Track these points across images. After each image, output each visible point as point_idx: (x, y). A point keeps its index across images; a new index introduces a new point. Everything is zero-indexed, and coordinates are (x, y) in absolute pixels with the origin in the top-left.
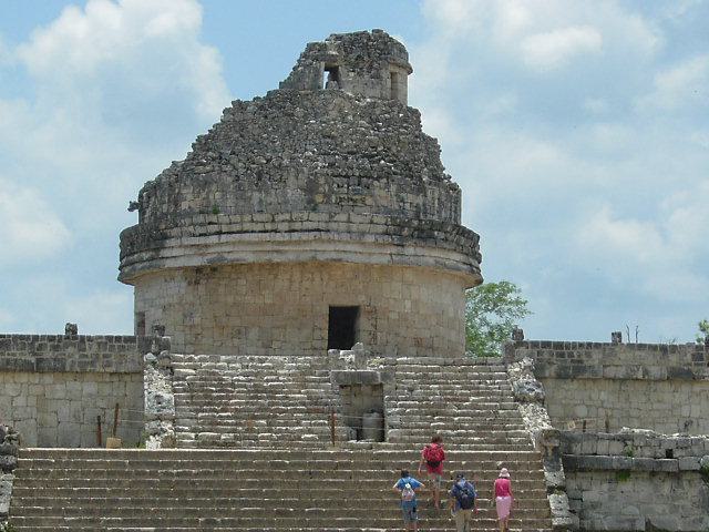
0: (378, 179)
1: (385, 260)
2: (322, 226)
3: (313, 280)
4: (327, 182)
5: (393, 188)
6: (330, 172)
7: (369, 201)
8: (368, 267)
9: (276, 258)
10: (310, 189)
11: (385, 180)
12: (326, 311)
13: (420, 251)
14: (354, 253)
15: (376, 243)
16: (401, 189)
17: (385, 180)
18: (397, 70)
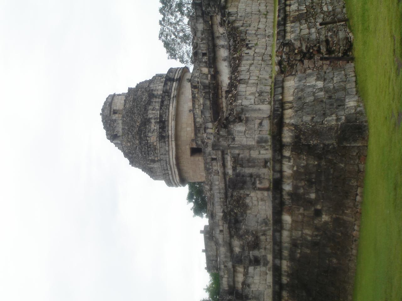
0: (147, 140)
1: (174, 143)
2: (165, 162)
3: (183, 161)
4: (151, 157)
5: (150, 134)
6: (147, 156)
7: (155, 144)
8: (177, 146)
10: (153, 161)
11: (148, 138)
12: (192, 158)
13: (170, 128)
15: (169, 146)
17: (148, 138)
18: (112, 110)
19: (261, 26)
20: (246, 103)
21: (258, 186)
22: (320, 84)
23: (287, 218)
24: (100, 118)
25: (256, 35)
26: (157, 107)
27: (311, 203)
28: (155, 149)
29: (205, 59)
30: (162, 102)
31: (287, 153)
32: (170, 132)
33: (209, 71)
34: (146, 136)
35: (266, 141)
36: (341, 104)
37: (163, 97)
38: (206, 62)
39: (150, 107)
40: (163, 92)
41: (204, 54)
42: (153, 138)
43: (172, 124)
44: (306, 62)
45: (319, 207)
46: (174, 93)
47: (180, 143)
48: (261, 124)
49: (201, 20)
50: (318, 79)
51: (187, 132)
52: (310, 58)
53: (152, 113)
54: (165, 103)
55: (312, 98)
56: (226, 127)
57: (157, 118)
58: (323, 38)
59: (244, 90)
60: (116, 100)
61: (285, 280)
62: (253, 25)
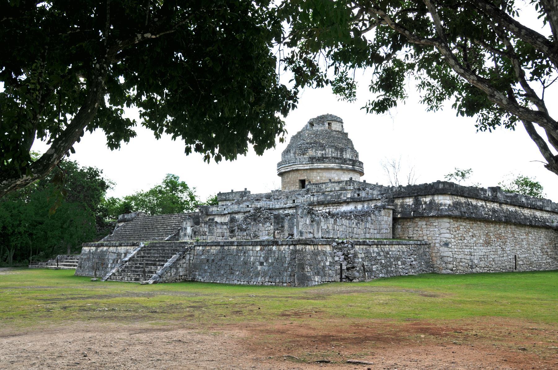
1: (308, 167)
5: (314, 150)
8: (307, 169)
9: (287, 170)
10: (295, 153)
12: (298, 181)
13: (318, 164)
14: (301, 167)
16: (316, 150)
19: (372, 231)
20: (322, 224)
21: (276, 232)
22: (328, 264)
23: (258, 248)
24: (325, 113)
25: (365, 228)
26: (333, 155)
27: (267, 260)
28: (304, 154)
29: (356, 195)
30: (337, 158)
31: (291, 247)
32: (316, 164)
33: (348, 198)
34: (312, 147)
35: (301, 236)
36: (318, 274)
37: (340, 159)
38: (354, 196)
39: (333, 150)
40: (345, 159)
41: (359, 195)
42: (311, 153)
43: (322, 166)
44: (343, 257)
45: (265, 264)
46: (344, 166)
47: (309, 171)
48: (310, 233)
49: (379, 193)
50: (330, 262)
51: (316, 177)
52: (345, 259)
53: (329, 152)
54: (337, 161)
55: (320, 259)
56: (308, 213)
57: (325, 154)
58: (356, 265)
59: (330, 222)
60: (338, 124)
61: (226, 248)
62: (372, 226)
